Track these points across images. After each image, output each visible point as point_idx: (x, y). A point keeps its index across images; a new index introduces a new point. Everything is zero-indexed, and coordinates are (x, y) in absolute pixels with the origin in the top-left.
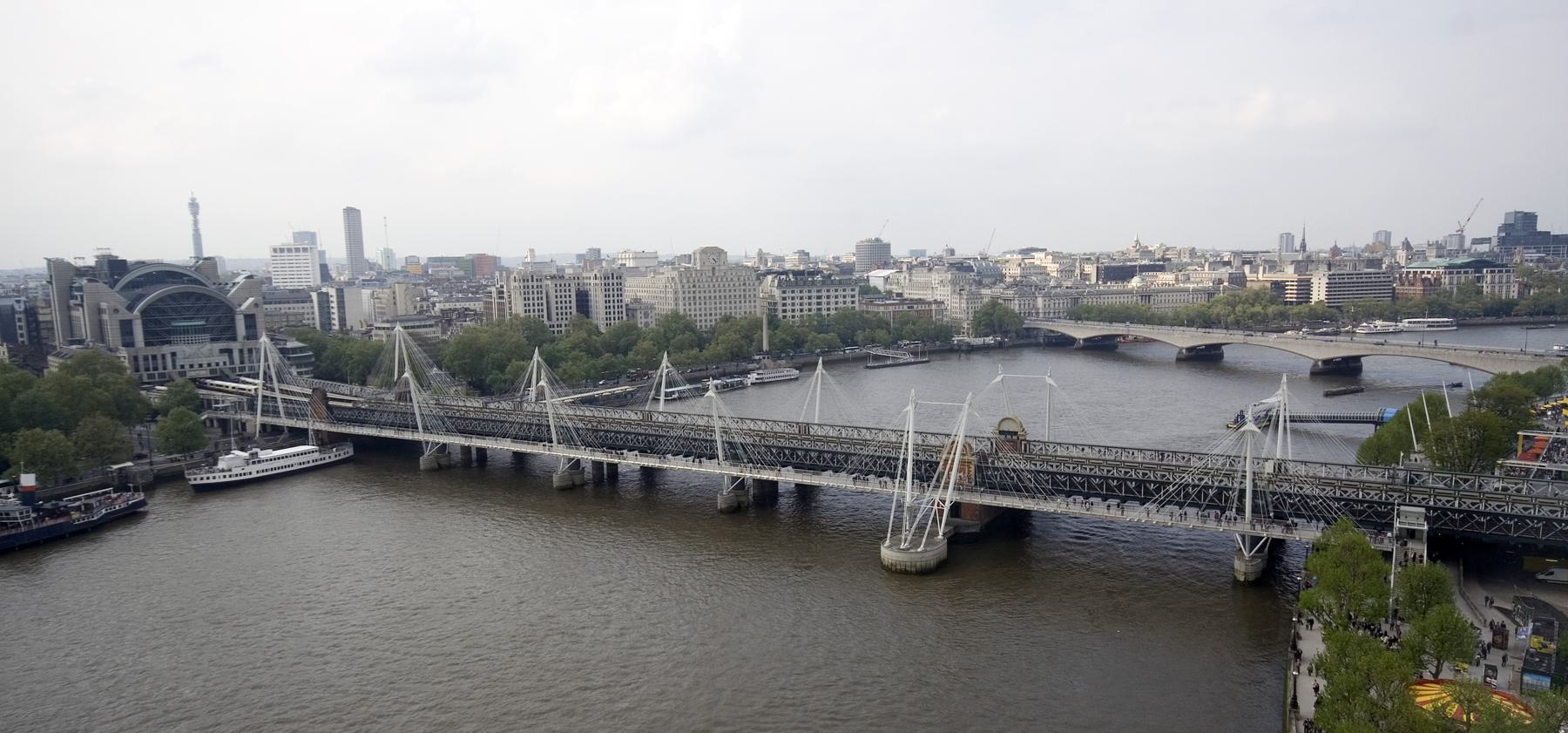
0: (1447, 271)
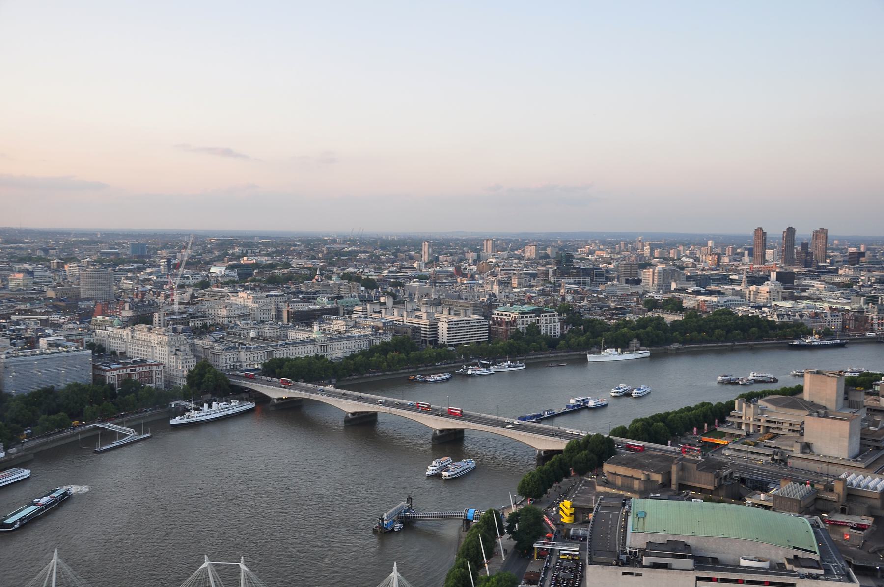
0: (520, 316)
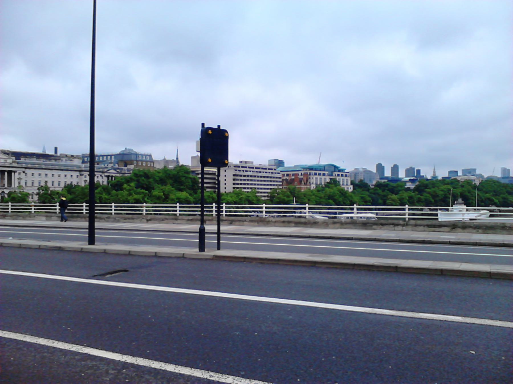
0: (313, 172)
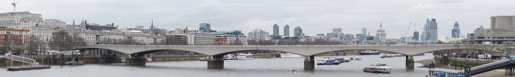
0: (229, 35)
